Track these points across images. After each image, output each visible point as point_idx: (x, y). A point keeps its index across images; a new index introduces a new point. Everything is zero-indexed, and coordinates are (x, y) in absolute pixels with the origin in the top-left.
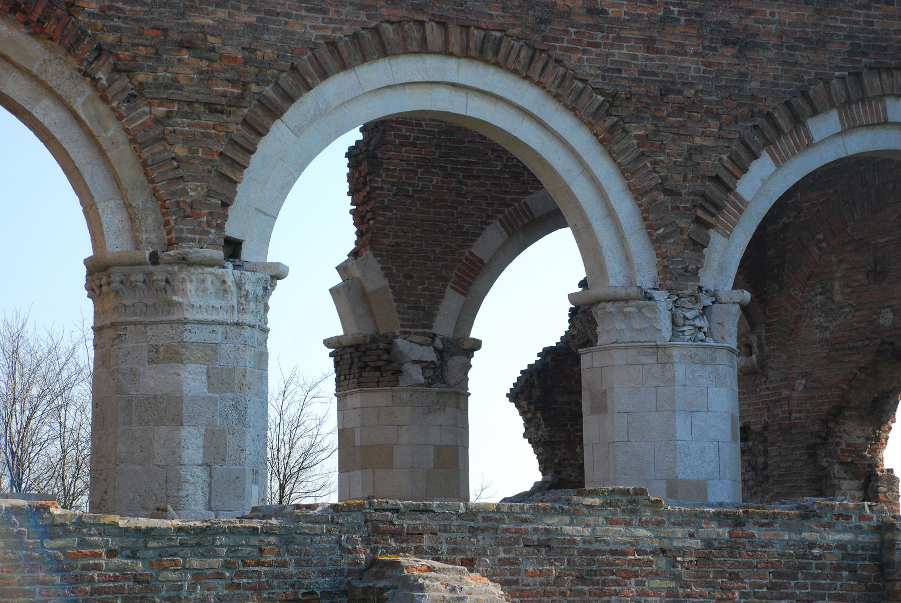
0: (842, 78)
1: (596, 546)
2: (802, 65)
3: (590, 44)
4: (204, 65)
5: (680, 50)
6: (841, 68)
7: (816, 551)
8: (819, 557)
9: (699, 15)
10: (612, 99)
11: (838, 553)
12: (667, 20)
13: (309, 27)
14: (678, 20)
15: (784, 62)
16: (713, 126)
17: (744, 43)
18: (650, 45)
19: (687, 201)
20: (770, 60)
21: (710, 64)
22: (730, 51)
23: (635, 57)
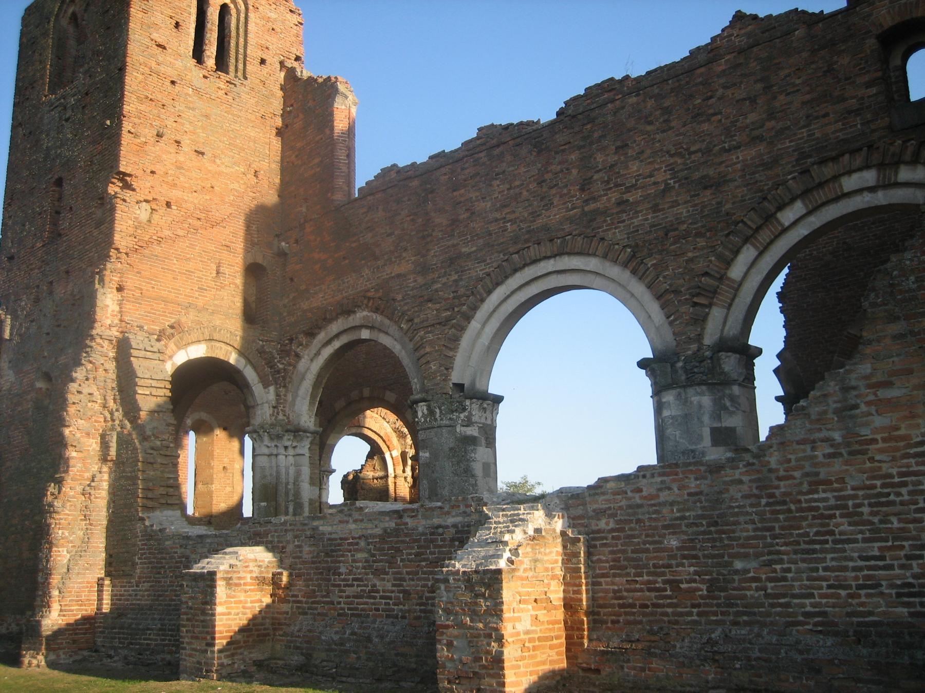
0: (794, 178)
1: (333, 536)
2: (761, 181)
3: (619, 222)
4: (438, 306)
5: (675, 204)
6: (790, 173)
7: (440, 530)
8: (442, 534)
9: (686, 178)
10: (636, 248)
11: (453, 530)
12: (668, 189)
13: (479, 270)
14: (673, 187)
15: (748, 184)
16: (701, 242)
17: (716, 184)
18: (655, 209)
19: (685, 295)
20: (737, 187)
21: (695, 205)
22: (708, 192)
23: (647, 219)
